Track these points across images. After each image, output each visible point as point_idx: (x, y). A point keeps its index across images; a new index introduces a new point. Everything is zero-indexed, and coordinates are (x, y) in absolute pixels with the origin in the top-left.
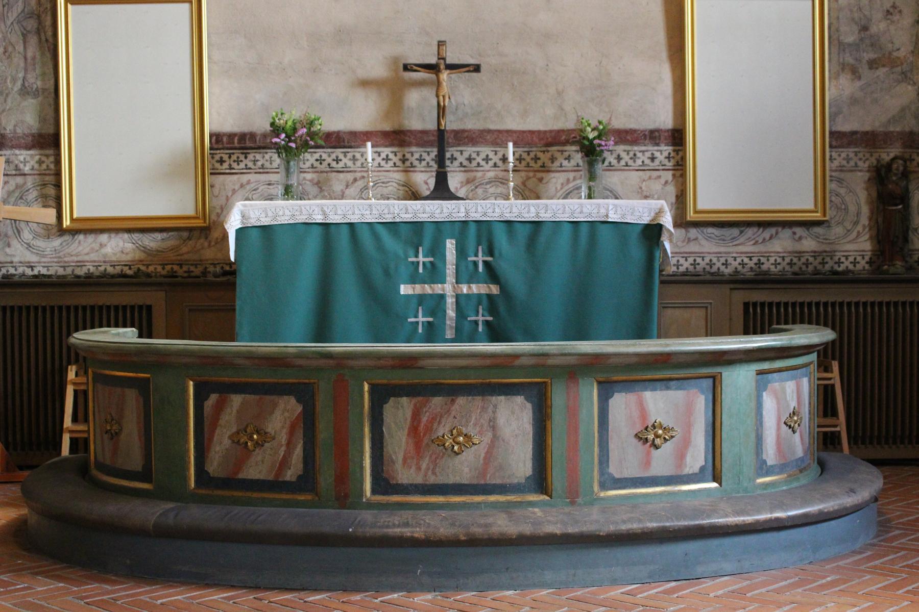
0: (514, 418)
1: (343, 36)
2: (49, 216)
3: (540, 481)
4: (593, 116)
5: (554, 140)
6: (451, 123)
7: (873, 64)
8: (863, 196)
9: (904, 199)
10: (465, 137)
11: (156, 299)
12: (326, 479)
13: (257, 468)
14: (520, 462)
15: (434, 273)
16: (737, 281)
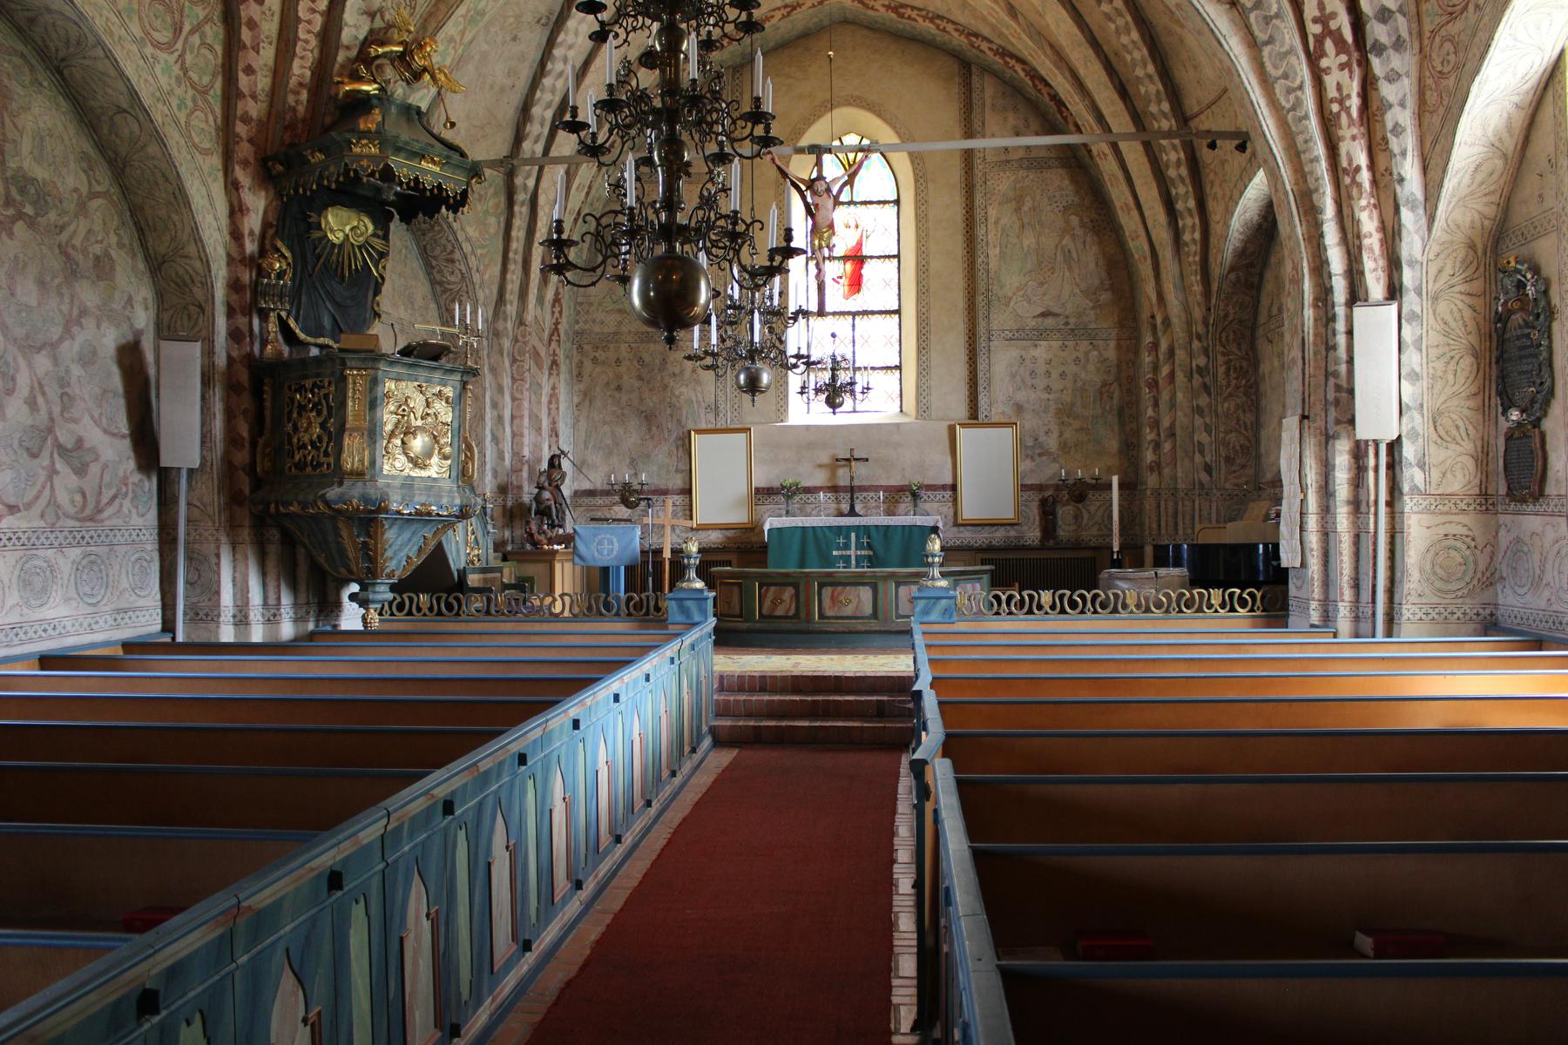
0: (866, 594)
1: (811, 446)
3: (875, 615)
4: (915, 479)
5: (901, 489)
6: (856, 483)
7: (1040, 455)
9: (1054, 514)
11: (733, 558)
12: (803, 615)
13: (780, 612)
14: (868, 610)
15: (847, 546)
16: (979, 550)
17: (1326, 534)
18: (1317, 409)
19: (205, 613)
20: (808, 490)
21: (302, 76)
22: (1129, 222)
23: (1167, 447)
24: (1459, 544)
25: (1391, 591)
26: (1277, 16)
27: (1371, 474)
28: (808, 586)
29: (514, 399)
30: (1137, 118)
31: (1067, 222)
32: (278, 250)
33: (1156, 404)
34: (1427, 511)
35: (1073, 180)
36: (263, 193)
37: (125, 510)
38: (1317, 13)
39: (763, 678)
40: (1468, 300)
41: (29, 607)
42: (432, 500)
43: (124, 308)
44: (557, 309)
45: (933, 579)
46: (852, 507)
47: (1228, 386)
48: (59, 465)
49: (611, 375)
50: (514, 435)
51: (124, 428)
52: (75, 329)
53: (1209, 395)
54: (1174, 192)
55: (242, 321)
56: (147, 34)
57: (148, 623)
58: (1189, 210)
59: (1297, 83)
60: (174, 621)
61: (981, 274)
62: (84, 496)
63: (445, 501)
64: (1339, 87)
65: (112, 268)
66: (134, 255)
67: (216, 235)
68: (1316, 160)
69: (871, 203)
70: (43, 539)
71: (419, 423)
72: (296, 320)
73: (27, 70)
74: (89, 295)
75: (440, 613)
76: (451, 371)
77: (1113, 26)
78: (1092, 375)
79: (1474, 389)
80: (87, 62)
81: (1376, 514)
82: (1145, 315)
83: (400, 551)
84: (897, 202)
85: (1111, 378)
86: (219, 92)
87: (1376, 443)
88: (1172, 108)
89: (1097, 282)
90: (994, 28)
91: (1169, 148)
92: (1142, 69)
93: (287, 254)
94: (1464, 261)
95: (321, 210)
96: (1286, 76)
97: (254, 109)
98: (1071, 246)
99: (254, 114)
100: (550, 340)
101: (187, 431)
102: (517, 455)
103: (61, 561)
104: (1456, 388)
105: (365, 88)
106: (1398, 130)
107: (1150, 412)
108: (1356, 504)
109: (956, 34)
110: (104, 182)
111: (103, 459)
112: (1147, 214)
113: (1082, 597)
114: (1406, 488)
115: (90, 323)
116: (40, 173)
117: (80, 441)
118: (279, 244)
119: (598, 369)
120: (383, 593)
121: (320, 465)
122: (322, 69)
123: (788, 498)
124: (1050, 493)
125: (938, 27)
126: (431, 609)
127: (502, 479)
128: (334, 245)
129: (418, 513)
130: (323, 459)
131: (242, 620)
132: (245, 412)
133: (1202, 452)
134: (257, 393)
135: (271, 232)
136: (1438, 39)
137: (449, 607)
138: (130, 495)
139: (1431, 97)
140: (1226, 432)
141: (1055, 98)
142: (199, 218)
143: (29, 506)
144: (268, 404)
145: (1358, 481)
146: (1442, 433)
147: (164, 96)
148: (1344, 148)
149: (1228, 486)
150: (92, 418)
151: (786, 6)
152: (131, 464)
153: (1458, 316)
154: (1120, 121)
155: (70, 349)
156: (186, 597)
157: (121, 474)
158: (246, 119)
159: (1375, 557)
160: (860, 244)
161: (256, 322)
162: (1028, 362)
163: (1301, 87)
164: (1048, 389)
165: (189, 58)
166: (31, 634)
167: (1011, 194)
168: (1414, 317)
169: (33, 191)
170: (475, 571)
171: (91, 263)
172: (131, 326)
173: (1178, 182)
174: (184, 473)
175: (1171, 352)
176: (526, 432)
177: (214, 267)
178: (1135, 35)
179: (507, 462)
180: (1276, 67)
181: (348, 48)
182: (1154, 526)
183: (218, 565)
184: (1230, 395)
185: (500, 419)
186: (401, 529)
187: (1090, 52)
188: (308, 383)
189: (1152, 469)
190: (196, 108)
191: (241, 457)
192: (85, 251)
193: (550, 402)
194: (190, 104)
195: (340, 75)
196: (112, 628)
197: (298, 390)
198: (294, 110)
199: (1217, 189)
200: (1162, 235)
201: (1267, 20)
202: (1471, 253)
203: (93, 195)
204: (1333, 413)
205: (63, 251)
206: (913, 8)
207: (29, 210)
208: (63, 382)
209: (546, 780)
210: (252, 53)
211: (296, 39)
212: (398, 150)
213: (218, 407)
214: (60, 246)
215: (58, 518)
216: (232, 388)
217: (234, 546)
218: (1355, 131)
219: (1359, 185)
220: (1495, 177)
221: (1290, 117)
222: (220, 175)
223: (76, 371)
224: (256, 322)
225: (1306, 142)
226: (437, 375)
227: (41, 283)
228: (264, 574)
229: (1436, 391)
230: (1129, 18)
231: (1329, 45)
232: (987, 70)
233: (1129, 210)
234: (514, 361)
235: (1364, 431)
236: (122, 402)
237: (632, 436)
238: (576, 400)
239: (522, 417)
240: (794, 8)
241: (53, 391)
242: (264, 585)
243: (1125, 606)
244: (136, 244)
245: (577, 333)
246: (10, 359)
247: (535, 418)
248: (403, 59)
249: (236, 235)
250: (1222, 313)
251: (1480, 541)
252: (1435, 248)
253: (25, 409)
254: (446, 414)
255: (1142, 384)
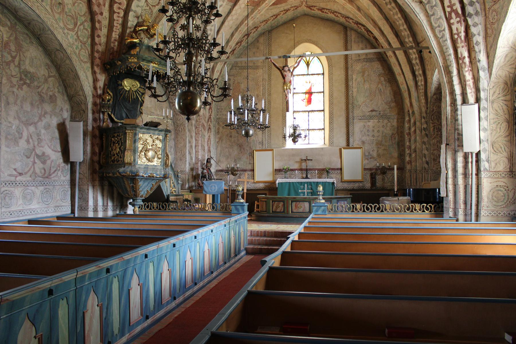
0: (307, 205)
1: (293, 155)
2: (253, 181)
4: (328, 166)
5: (323, 170)
6: (308, 168)
7: (371, 158)
8: (369, 177)
9: (375, 178)
10: (310, 170)
11: (267, 192)
12: (286, 211)
13: (278, 210)
15: (304, 189)
17: (455, 185)
18: (452, 142)
19: (84, 208)
20: (292, 170)
21: (116, 37)
22: (400, 79)
23: (413, 155)
24: (502, 189)
25: (477, 205)
26: (435, 6)
27: (470, 164)
28: (288, 202)
29: (196, 140)
30: (402, 43)
31: (380, 79)
32: (108, 93)
33: (410, 141)
34: (490, 177)
35: (382, 65)
36: (104, 75)
37: (59, 175)
38: (449, 4)
39: (265, 232)
40: (504, 102)
41: (26, 205)
42: (154, 172)
43: (60, 111)
44: (210, 111)
45: (320, 200)
46: (307, 176)
47: (434, 134)
48: (36, 161)
49: (228, 132)
50: (196, 152)
51: (59, 149)
52: (43, 118)
53: (428, 137)
54: (415, 68)
55: (97, 115)
56: (65, 26)
57: (66, 211)
58: (420, 74)
59: (443, 28)
60: (74, 210)
61: (350, 98)
62: (45, 170)
63: (158, 173)
64: (457, 29)
65: (56, 99)
66: (63, 95)
67: (89, 88)
68: (450, 55)
69: (314, 74)
70: (31, 184)
71: (151, 147)
72: (114, 115)
73: (28, 38)
74: (48, 107)
75: (160, 209)
76: (161, 131)
77: (392, 13)
78: (388, 131)
79: (507, 134)
80: (46, 35)
81: (472, 178)
82: (406, 110)
83: (145, 189)
84: (323, 74)
85: (395, 132)
86: (90, 43)
87: (472, 153)
88: (413, 40)
89: (390, 100)
90: (353, 15)
91: (412, 53)
92: (402, 27)
93: (111, 94)
94: (502, 89)
95: (122, 79)
96: (439, 26)
97: (100, 48)
98: (381, 87)
99: (100, 50)
100: (208, 121)
101: (79, 151)
102: (197, 158)
103: (36, 190)
104: (501, 133)
105: (135, 40)
106: (478, 43)
107: (408, 144)
108: (465, 175)
109: (341, 17)
110: (54, 72)
111: (51, 159)
112: (406, 76)
113: (371, 206)
114: (482, 169)
115: (48, 116)
116: (32, 70)
117: (44, 154)
118: (109, 91)
119: (224, 130)
120: (140, 202)
121: (119, 161)
122: (122, 36)
123: (285, 172)
124: (374, 171)
125: (335, 15)
126: (157, 208)
127: (192, 166)
128: (126, 91)
129: (149, 176)
130: (120, 159)
131: (95, 210)
132: (97, 144)
133: (425, 157)
134: (101, 138)
135: (106, 87)
136: (491, 11)
137: (163, 207)
138: (61, 170)
139: (489, 31)
140: (433, 150)
141: (375, 38)
142: (83, 83)
143: (26, 173)
144: (104, 142)
145: (466, 167)
146: (495, 150)
147: (71, 45)
148: (459, 50)
149: (434, 169)
150: (48, 146)
151: (285, 10)
152: (61, 160)
153: (501, 108)
154: (395, 44)
155: (41, 124)
156: (78, 203)
157: (58, 164)
158: (98, 52)
159: (471, 193)
160: (311, 88)
161: (101, 115)
162: (366, 127)
163: (444, 30)
164: (373, 136)
165: (79, 33)
166: (26, 213)
167: (360, 70)
168: (485, 109)
169: (29, 76)
170: (172, 196)
171: (48, 98)
172: (62, 117)
173: (416, 65)
174: (78, 163)
175: (415, 123)
176: (200, 151)
177: (88, 99)
178: (399, 15)
179: (194, 161)
180: (436, 23)
181: (130, 28)
182: (409, 182)
183: (88, 192)
184: (435, 137)
185: (191, 146)
186: (144, 182)
187: (385, 22)
188: (116, 135)
189: (408, 163)
190: (82, 48)
191: (96, 158)
192: (47, 94)
193: (208, 141)
194: (80, 47)
195: (128, 37)
196: (54, 212)
197: (114, 137)
198: (113, 48)
199: (429, 67)
200: (411, 83)
201: (432, 7)
202: (506, 86)
203: (50, 77)
204: (457, 143)
205: (39, 94)
206: (327, 9)
207: (28, 81)
208: (38, 135)
209: (159, 264)
210: (99, 31)
211: (114, 26)
212: (143, 60)
213: (89, 142)
214: (38, 92)
215: (36, 177)
216: (93, 136)
217: (94, 187)
218: (463, 44)
219: (465, 63)
220: (512, 60)
221: (441, 40)
222: (90, 69)
223: (43, 131)
224: (101, 115)
225: (446, 49)
226: (157, 132)
227: (32, 104)
228: (103, 196)
229: (493, 135)
230: (397, 10)
231: (453, 15)
232: (352, 29)
233: (400, 75)
234: (196, 128)
235: (466, 149)
236: (58, 141)
237: (235, 151)
238: (217, 140)
239: (198, 146)
240: (287, 11)
241: (35, 138)
242: (103, 199)
243: (386, 210)
244: (64, 92)
245: (217, 118)
246: (21, 128)
247: (203, 146)
248: (147, 31)
249: (95, 88)
250: (432, 110)
251: (510, 188)
252: (492, 85)
253: (26, 143)
254: (160, 145)
255: (405, 134)
